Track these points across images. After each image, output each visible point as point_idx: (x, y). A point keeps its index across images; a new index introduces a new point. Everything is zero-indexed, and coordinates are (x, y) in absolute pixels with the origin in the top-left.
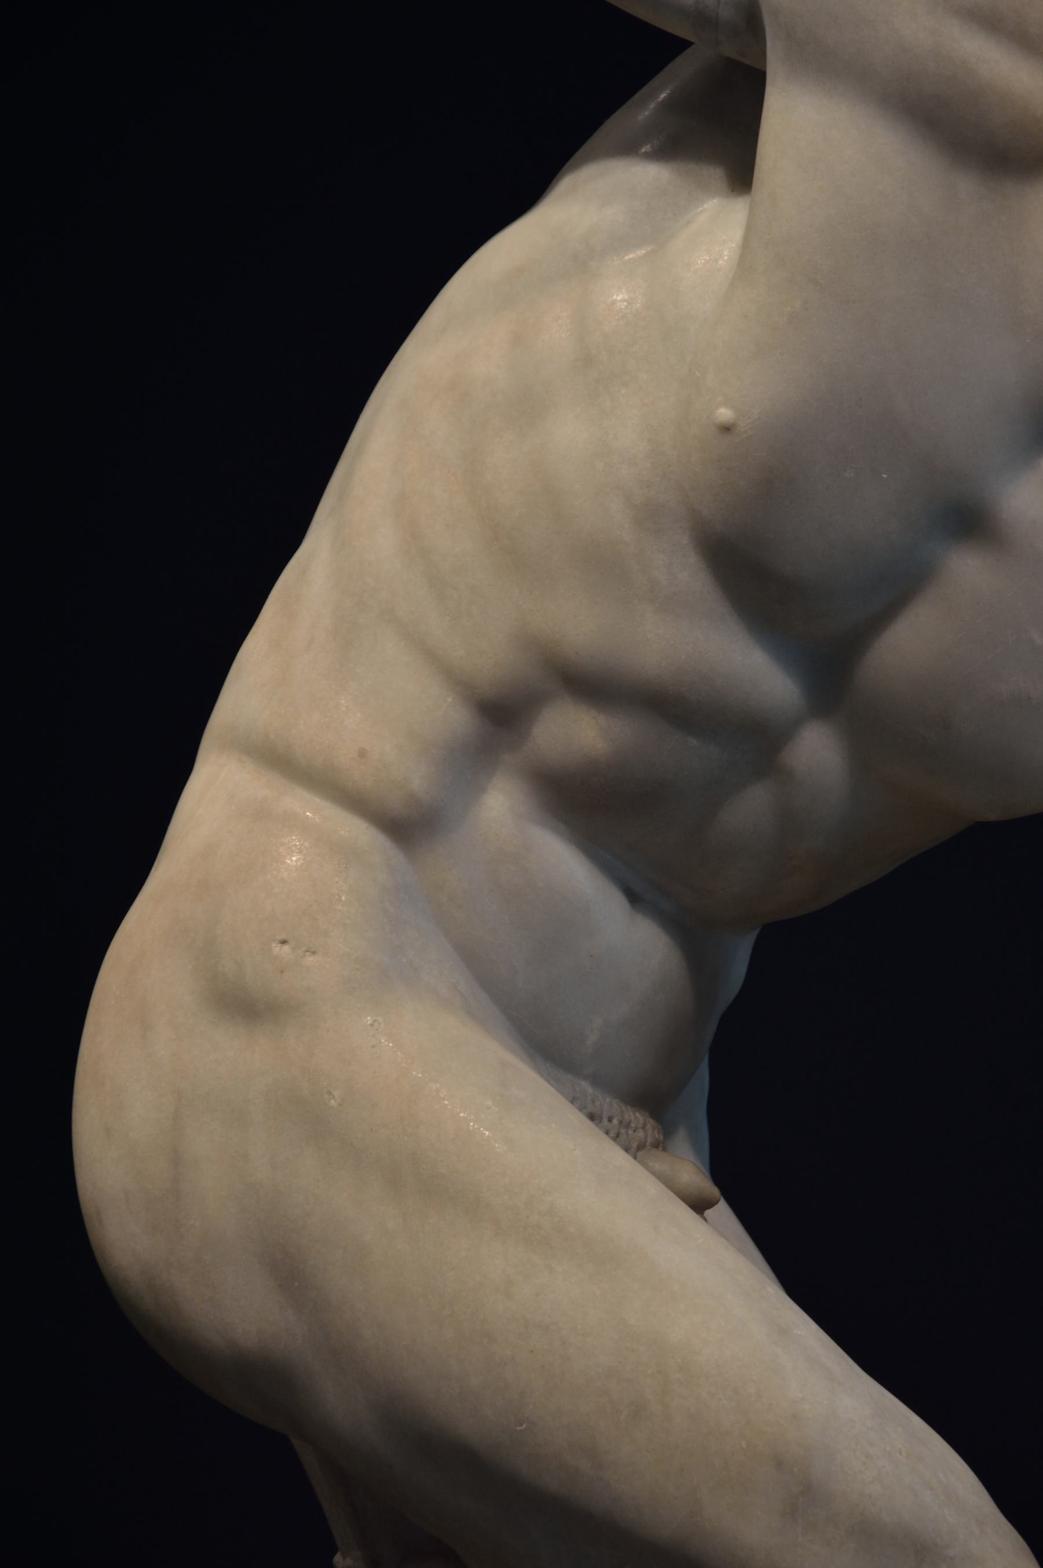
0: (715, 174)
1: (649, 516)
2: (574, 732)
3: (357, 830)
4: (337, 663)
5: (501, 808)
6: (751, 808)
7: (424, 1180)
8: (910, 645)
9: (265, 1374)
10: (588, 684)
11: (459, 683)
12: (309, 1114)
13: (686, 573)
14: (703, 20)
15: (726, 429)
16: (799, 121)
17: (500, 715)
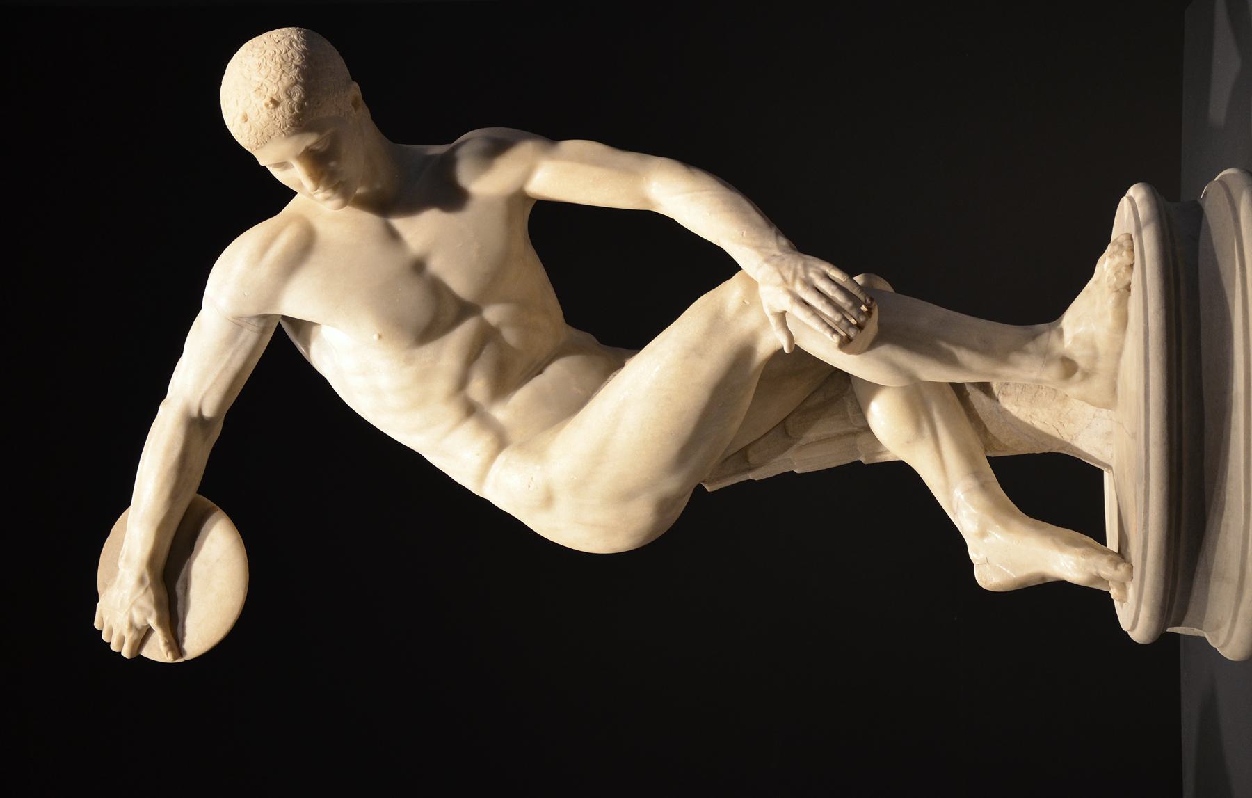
0: (315, 329)
1: (409, 361)
2: (478, 388)
3: (502, 458)
4: (457, 455)
5: (502, 413)
6: (510, 336)
7: (599, 455)
8: (459, 283)
9: (663, 505)
10: (462, 383)
11: (460, 422)
12: (580, 485)
13: (428, 350)
14: (263, 332)
15: (380, 337)
16: (294, 305)
17: (471, 410)
